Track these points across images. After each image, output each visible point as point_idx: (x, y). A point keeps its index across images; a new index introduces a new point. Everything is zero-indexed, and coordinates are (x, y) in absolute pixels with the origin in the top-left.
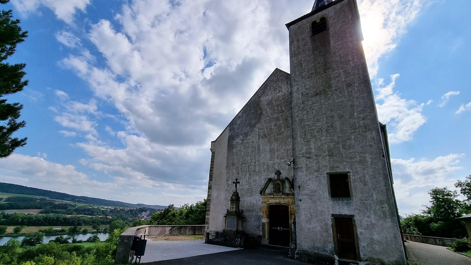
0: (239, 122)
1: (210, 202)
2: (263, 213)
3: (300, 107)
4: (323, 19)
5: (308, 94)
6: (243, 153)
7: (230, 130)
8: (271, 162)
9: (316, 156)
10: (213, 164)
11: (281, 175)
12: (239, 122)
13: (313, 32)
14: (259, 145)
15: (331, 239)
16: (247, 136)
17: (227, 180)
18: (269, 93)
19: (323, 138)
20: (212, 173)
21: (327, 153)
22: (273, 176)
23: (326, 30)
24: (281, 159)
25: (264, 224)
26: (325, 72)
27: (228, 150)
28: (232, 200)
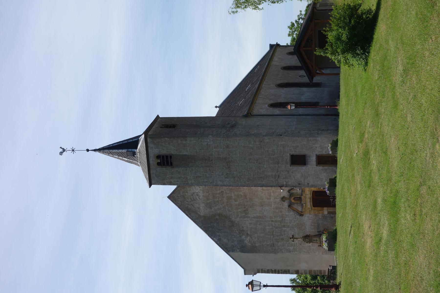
0: (225, 241)
1: (312, 270)
2: (319, 213)
3: (237, 180)
4: (158, 157)
5: (227, 174)
6: (262, 235)
7: (233, 251)
8: (273, 205)
9: (277, 172)
10: (271, 270)
11: (286, 196)
12: (225, 241)
13: (168, 165)
14: (255, 217)
15: (330, 168)
16: (243, 231)
17: (290, 252)
18: (197, 205)
19: (265, 166)
20: (281, 270)
21: (276, 165)
22: (286, 204)
23: (171, 157)
24: (270, 196)
25: (329, 213)
26: (212, 160)
27: (256, 252)
28: (310, 241)
